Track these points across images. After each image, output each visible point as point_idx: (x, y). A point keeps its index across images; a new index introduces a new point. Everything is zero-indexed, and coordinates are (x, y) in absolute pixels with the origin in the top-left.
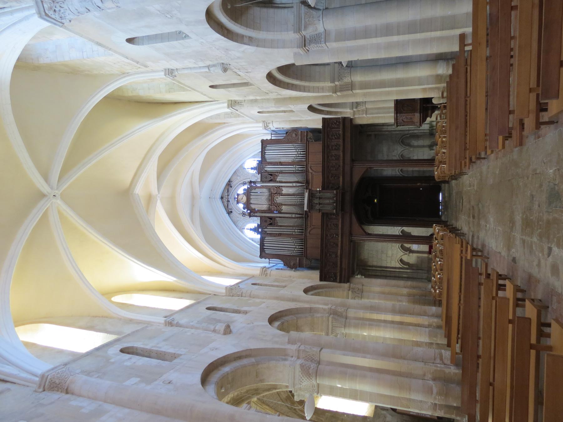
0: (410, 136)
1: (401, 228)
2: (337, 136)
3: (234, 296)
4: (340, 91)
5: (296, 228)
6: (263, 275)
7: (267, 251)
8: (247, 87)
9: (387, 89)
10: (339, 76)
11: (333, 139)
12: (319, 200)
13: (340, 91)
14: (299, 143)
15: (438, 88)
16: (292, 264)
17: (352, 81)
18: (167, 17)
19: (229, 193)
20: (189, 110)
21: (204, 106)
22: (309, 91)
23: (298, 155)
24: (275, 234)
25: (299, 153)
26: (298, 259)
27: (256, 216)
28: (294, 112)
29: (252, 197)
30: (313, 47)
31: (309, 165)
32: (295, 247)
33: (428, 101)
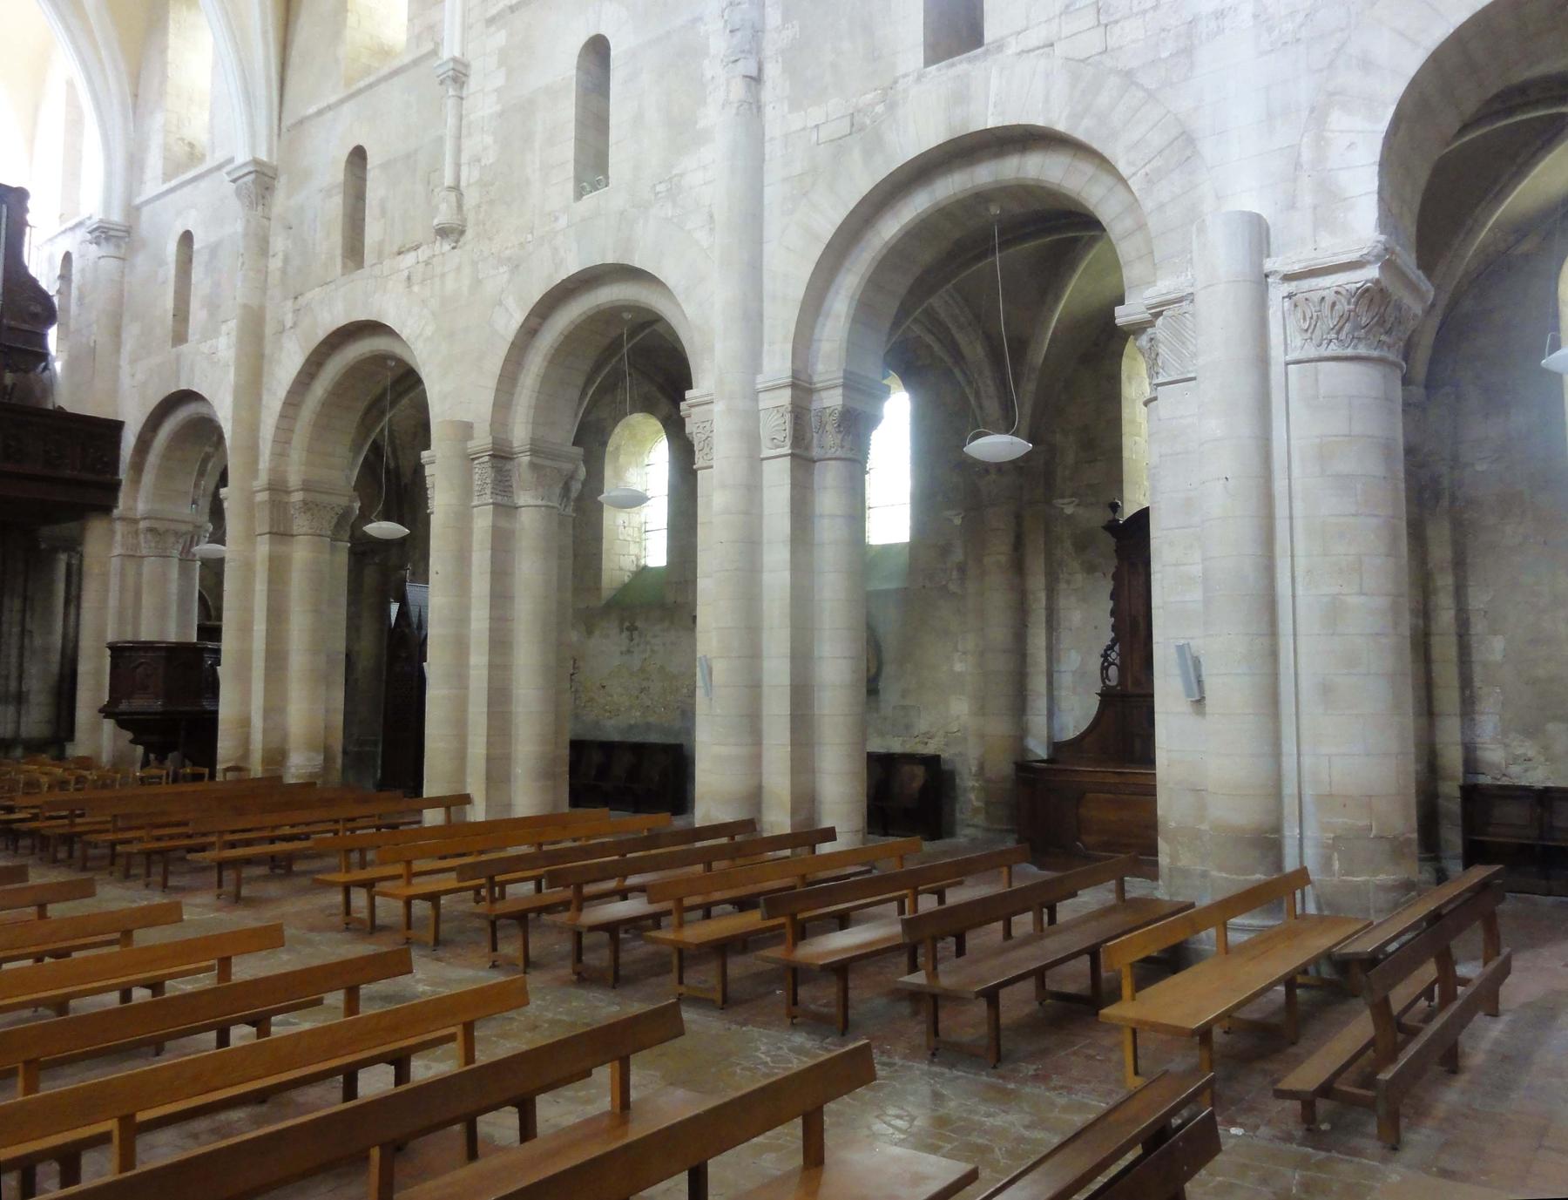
8: (338, 252)
10: (317, 505)
15: (246, 755)
17: (292, 536)
18: (660, 183)
20: (265, 33)
21: (269, 86)
22: (283, 416)
30: (482, 473)
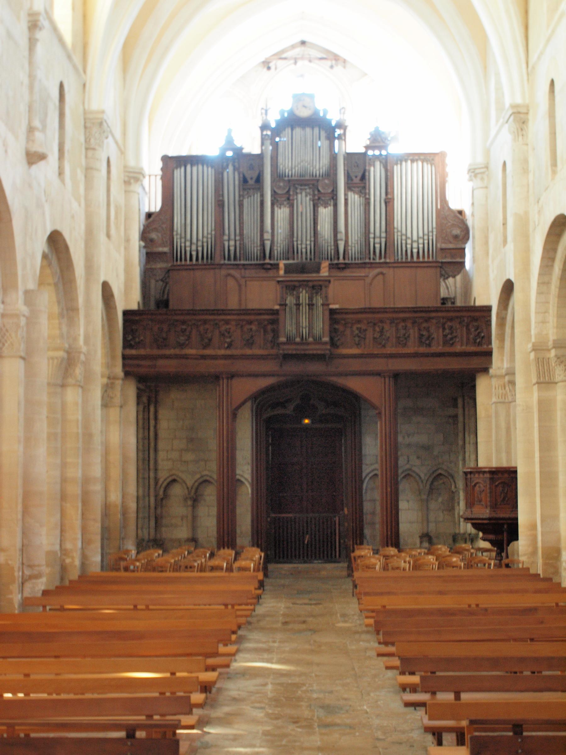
0: (453, 492)
1: (246, 479)
2: (452, 339)
3: (85, 132)
4: (537, 360)
5: (238, 243)
6: (127, 174)
7: (178, 174)
9: (537, 455)
11: (444, 329)
12: (306, 304)
13: (538, 359)
14: (439, 246)
16: (154, 235)
19: (317, 61)
22: (539, 293)
23: (409, 241)
24: (223, 191)
25: (415, 245)
26: (166, 249)
27: (262, 144)
28: (504, 245)
29: (308, 130)
31: (384, 271)
32: (194, 240)
33: (514, 535)
